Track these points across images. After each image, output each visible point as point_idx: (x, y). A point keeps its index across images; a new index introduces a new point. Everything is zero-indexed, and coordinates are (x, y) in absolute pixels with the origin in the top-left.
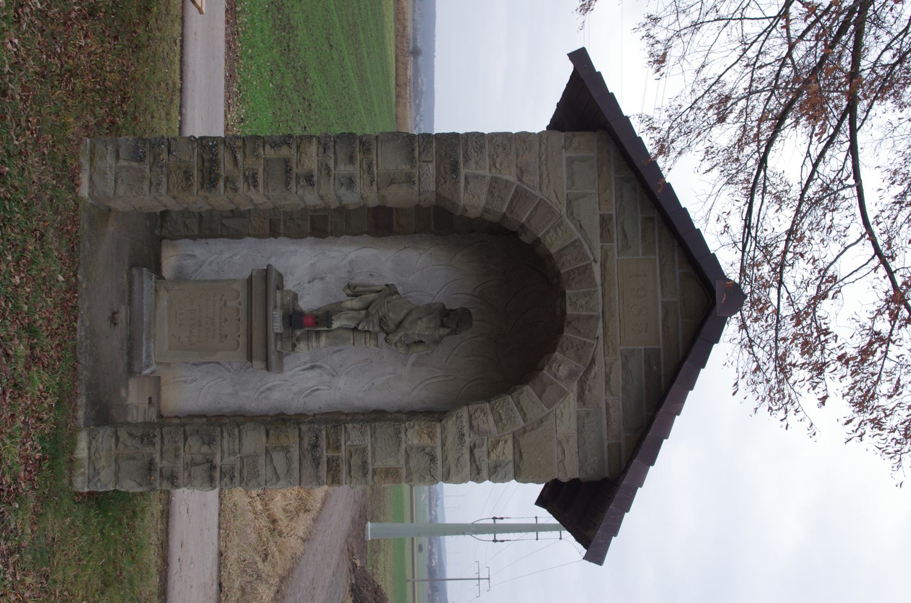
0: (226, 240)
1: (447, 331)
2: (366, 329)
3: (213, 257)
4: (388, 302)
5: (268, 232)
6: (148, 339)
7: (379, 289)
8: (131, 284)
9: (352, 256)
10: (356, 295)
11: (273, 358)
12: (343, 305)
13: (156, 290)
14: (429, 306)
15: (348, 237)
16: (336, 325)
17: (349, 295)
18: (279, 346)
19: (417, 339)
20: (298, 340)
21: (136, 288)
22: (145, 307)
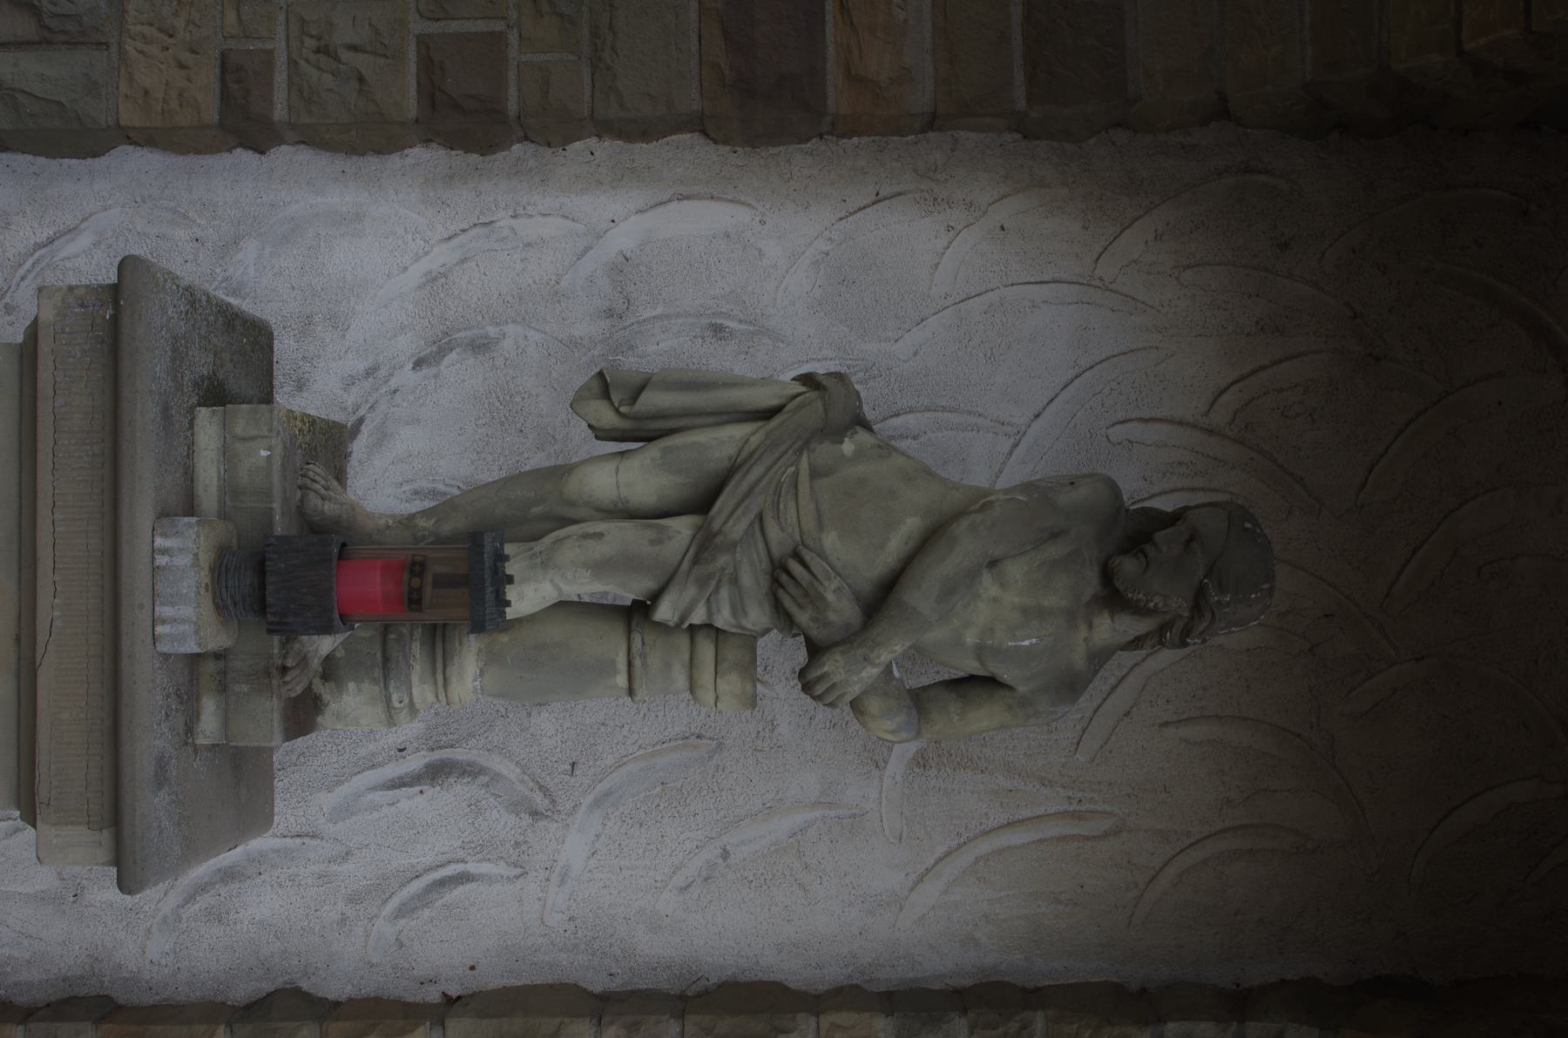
0: (21, 160)
1: (1130, 626)
2: (698, 617)
4: (815, 474)
5: (212, 115)
7: (764, 398)
9: (624, 239)
10: (642, 432)
11: (152, 808)
12: (572, 487)
14: (1037, 493)
15: (606, 148)
16: (525, 598)
17: (602, 434)
18: (209, 724)
19: (971, 666)
20: (330, 670)
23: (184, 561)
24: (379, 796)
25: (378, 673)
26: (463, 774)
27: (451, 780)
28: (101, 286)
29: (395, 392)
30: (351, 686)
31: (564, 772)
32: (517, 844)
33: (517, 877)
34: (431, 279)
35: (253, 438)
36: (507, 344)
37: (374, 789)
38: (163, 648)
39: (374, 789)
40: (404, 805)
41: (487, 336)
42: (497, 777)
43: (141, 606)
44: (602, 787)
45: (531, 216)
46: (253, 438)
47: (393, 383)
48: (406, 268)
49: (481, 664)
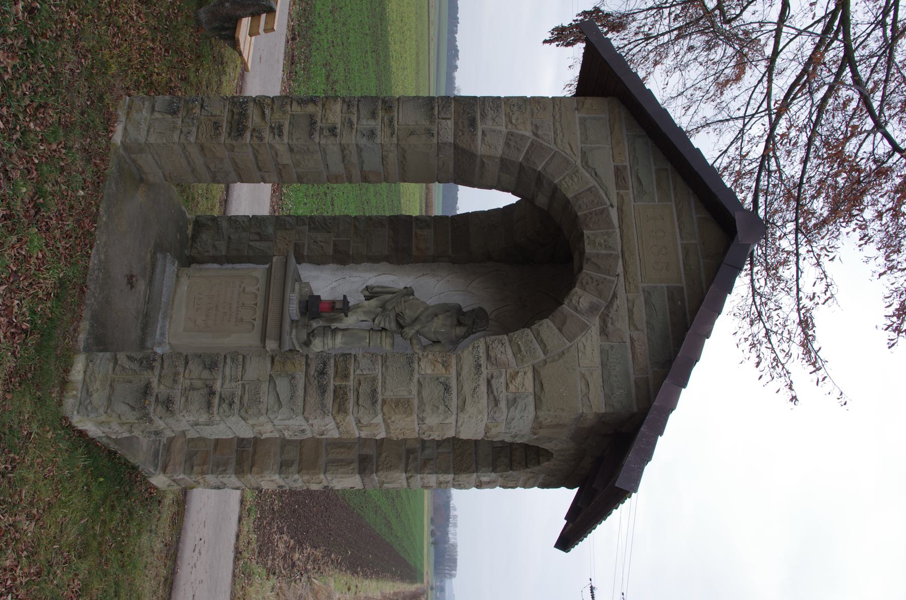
2: (382, 325)
6: (164, 318)
15: (368, 265)
21: (158, 270)
22: (165, 289)
34: (332, 288)
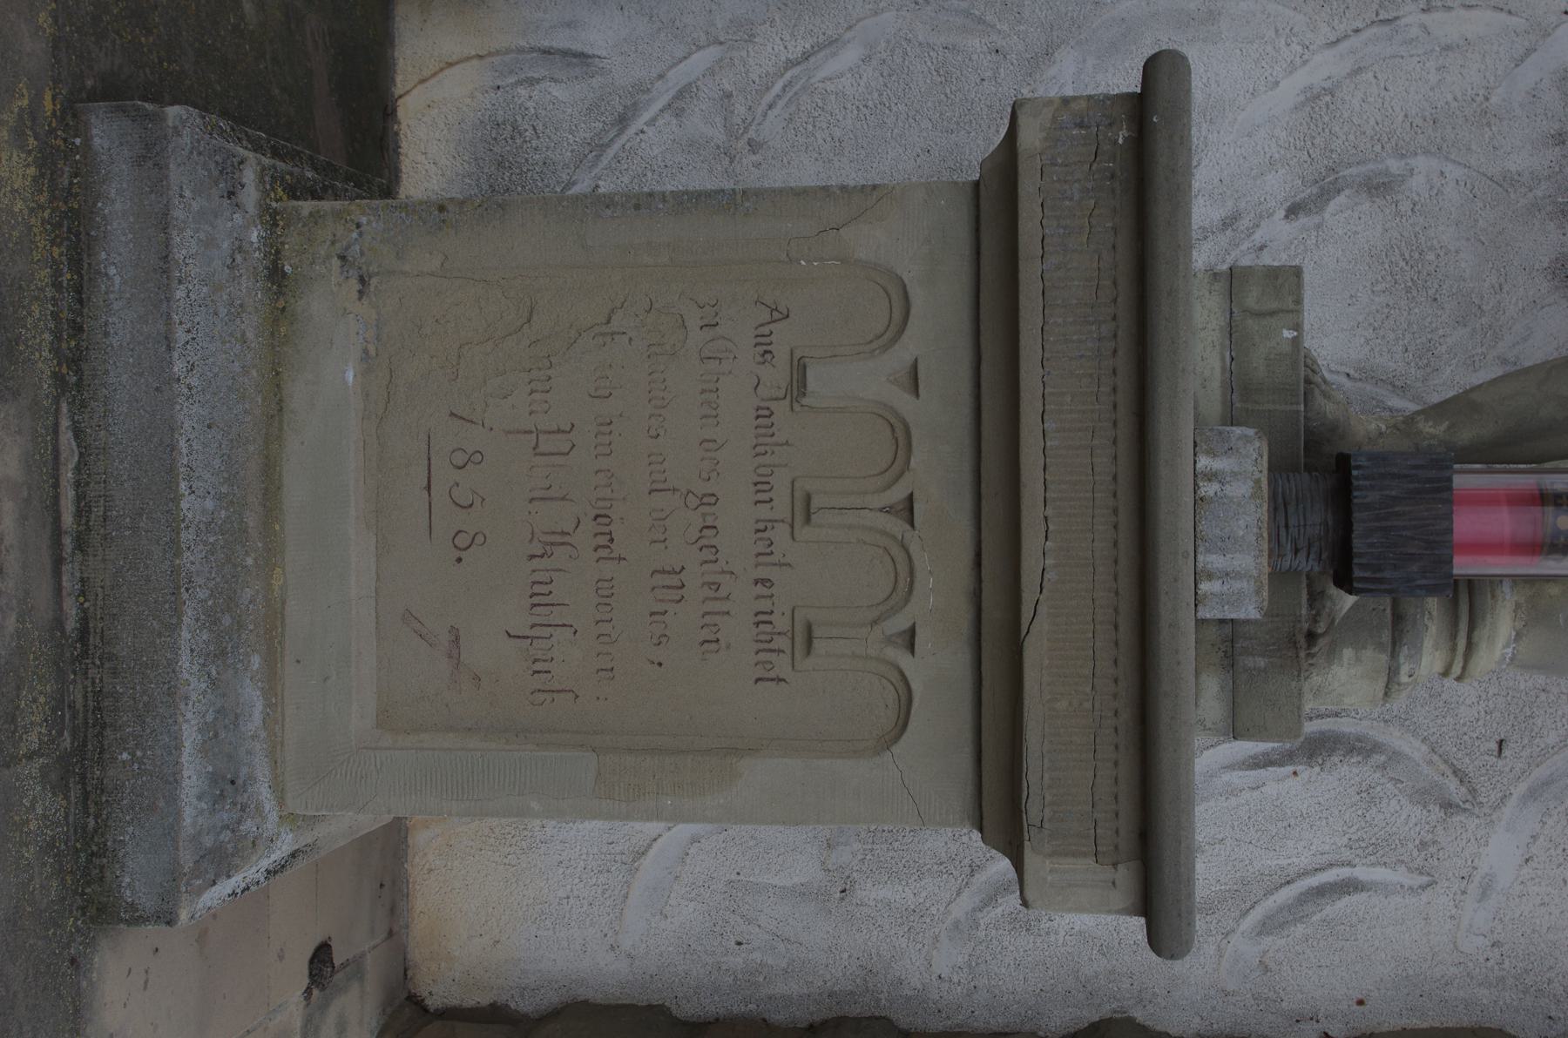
3: (701, 60)
6: (220, 654)
8: (75, 230)
13: (275, 275)
22: (189, 416)
23: (1239, 490)
24: (1236, 778)
25: (1386, 636)
26: (1351, 750)
27: (1336, 759)
28: (1107, 97)
29: (1261, 248)
30: (1348, 653)
31: (1488, 753)
32: (1423, 845)
33: (1423, 888)
35: (1272, 313)
36: (1417, 183)
37: (1231, 767)
38: (1205, 613)
39: (1231, 767)
40: (1271, 789)
41: (1387, 173)
42: (1396, 756)
43: (1186, 556)
44: (1540, 773)
45: (1450, 8)
46: (1272, 313)
47: (1258, 237)
48: (1277, 83)
49: (1519, 624)
